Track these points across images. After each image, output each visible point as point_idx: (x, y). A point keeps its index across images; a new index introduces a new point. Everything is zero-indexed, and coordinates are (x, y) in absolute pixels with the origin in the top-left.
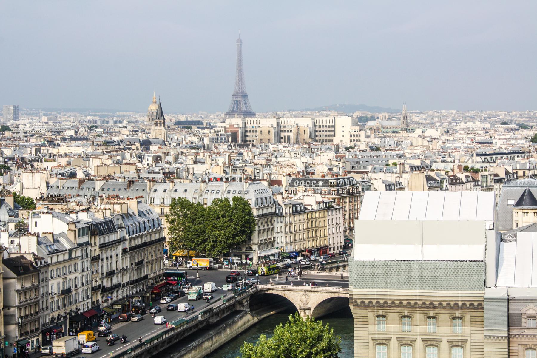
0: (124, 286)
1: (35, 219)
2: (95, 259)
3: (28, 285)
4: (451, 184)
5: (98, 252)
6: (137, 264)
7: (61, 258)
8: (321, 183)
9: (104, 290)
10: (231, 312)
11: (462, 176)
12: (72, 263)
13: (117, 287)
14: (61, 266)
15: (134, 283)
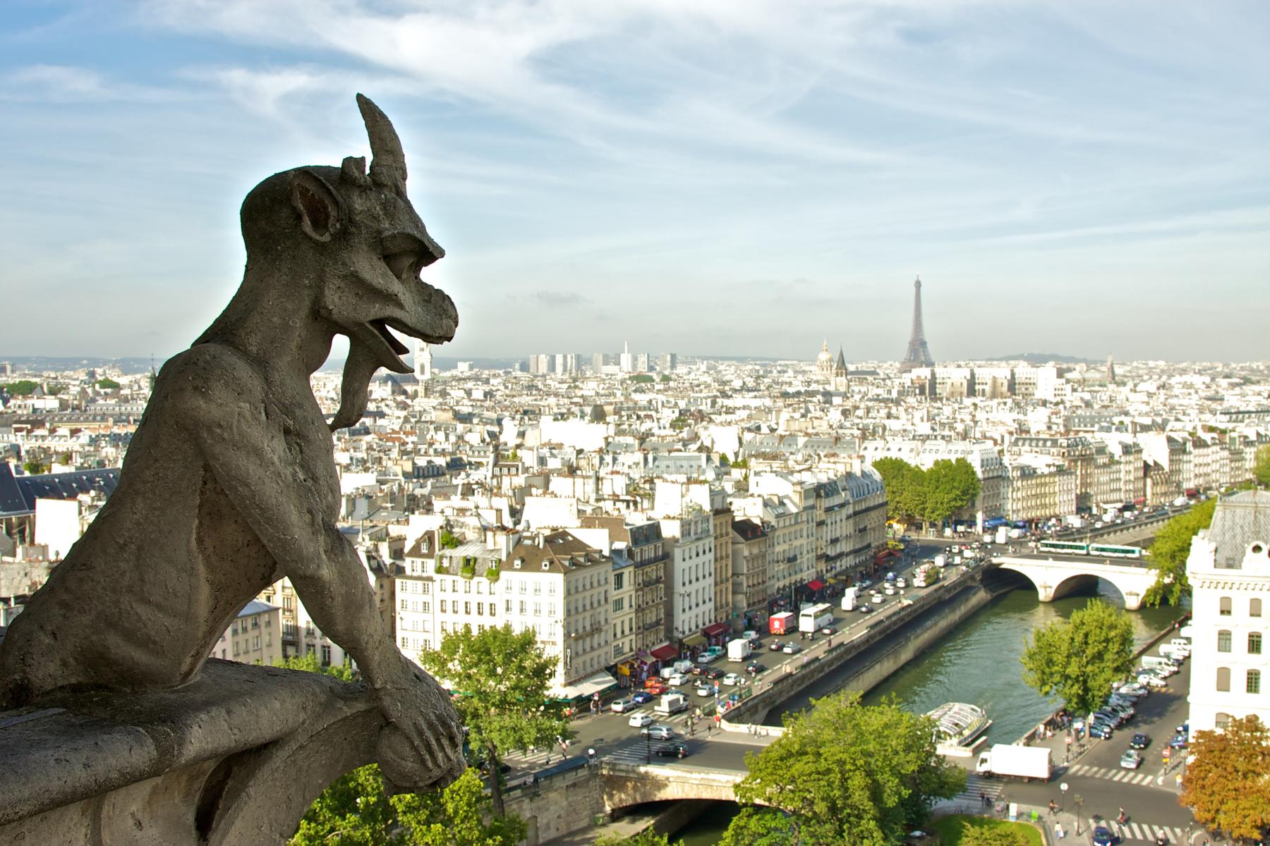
0: (848, 554)
1: (758, 478)
2: (821, 524)
3: (755, 551)
4: (1195, 446)
5: (824, 517)
6: (860, 531)
7: (787, 523)
8: (1049, 443)
9: (828, 559)
10: (962, 589)
11: (1207, 437)
12: (798, 527)
13: (840, 556)
14: (787, 531)
15: (856, 552)
